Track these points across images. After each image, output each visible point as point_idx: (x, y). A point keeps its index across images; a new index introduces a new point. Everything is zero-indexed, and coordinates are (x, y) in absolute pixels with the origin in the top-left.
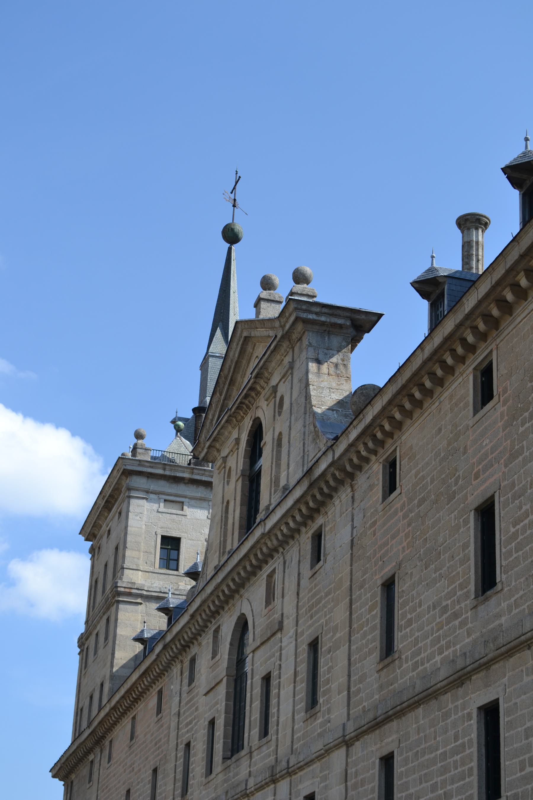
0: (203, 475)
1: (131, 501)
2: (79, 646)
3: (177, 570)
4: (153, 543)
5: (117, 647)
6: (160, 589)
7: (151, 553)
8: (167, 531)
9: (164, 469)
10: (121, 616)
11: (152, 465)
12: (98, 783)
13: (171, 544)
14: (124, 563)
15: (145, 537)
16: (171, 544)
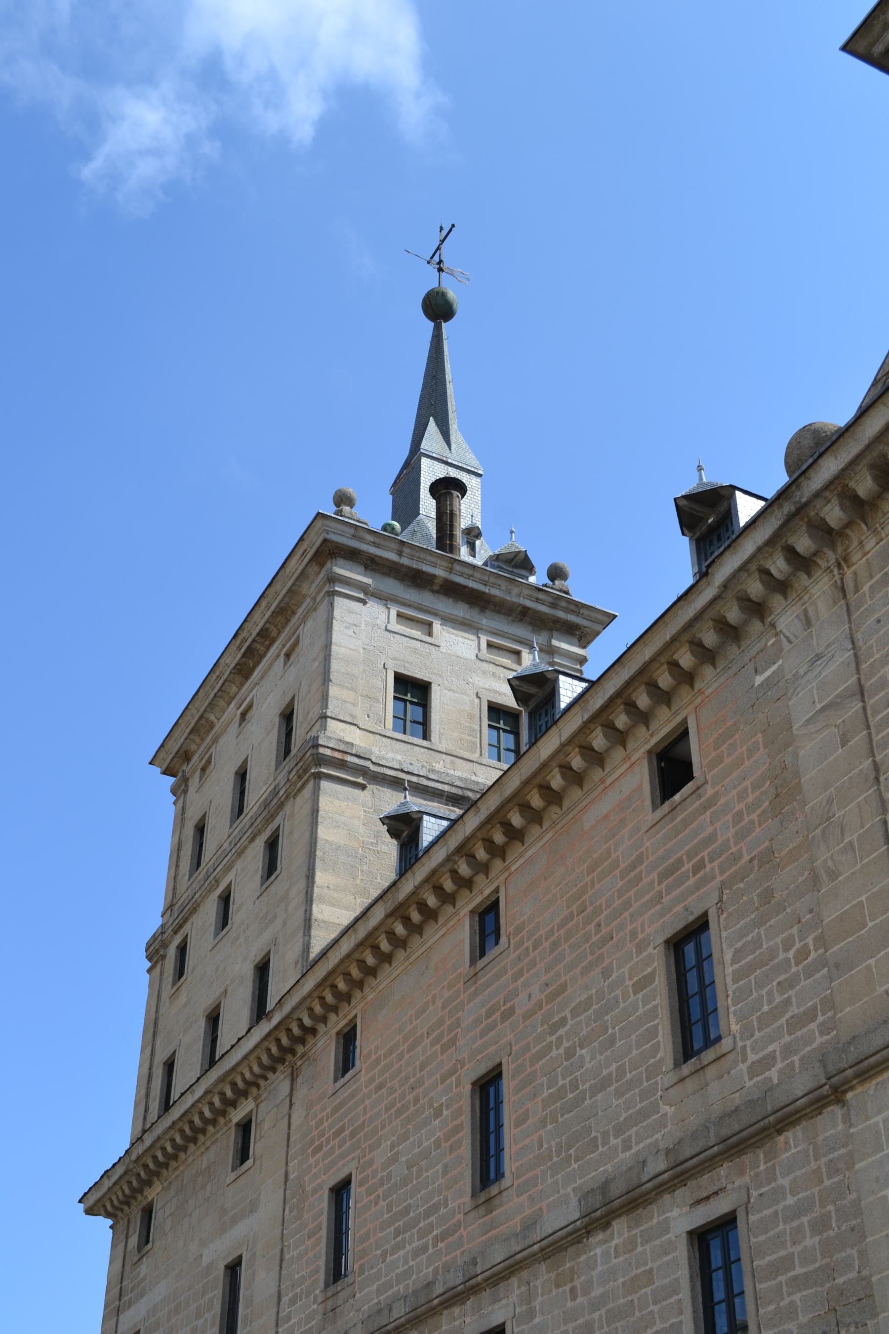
0: (469, 577)
1: (336, 601)
2: (149, 958)
3: (426, 736)
4: (380, 684)
5: (318, 863)
6: (400, 764)
7: (376, 700)
8: (405, 666)
9: (400, 554)
10: (324, 803)
11: (377, 540)
12: (288, 1146)
13: (413, 691)
14: (327, 708)
15: (364, 671)
16: (413, 691)
